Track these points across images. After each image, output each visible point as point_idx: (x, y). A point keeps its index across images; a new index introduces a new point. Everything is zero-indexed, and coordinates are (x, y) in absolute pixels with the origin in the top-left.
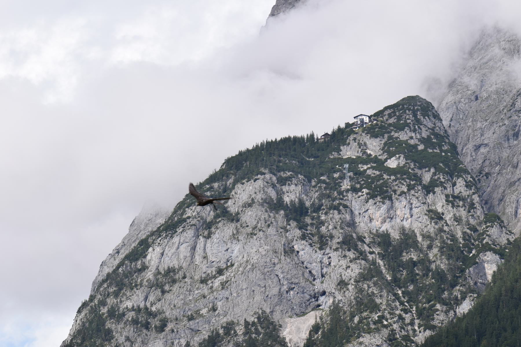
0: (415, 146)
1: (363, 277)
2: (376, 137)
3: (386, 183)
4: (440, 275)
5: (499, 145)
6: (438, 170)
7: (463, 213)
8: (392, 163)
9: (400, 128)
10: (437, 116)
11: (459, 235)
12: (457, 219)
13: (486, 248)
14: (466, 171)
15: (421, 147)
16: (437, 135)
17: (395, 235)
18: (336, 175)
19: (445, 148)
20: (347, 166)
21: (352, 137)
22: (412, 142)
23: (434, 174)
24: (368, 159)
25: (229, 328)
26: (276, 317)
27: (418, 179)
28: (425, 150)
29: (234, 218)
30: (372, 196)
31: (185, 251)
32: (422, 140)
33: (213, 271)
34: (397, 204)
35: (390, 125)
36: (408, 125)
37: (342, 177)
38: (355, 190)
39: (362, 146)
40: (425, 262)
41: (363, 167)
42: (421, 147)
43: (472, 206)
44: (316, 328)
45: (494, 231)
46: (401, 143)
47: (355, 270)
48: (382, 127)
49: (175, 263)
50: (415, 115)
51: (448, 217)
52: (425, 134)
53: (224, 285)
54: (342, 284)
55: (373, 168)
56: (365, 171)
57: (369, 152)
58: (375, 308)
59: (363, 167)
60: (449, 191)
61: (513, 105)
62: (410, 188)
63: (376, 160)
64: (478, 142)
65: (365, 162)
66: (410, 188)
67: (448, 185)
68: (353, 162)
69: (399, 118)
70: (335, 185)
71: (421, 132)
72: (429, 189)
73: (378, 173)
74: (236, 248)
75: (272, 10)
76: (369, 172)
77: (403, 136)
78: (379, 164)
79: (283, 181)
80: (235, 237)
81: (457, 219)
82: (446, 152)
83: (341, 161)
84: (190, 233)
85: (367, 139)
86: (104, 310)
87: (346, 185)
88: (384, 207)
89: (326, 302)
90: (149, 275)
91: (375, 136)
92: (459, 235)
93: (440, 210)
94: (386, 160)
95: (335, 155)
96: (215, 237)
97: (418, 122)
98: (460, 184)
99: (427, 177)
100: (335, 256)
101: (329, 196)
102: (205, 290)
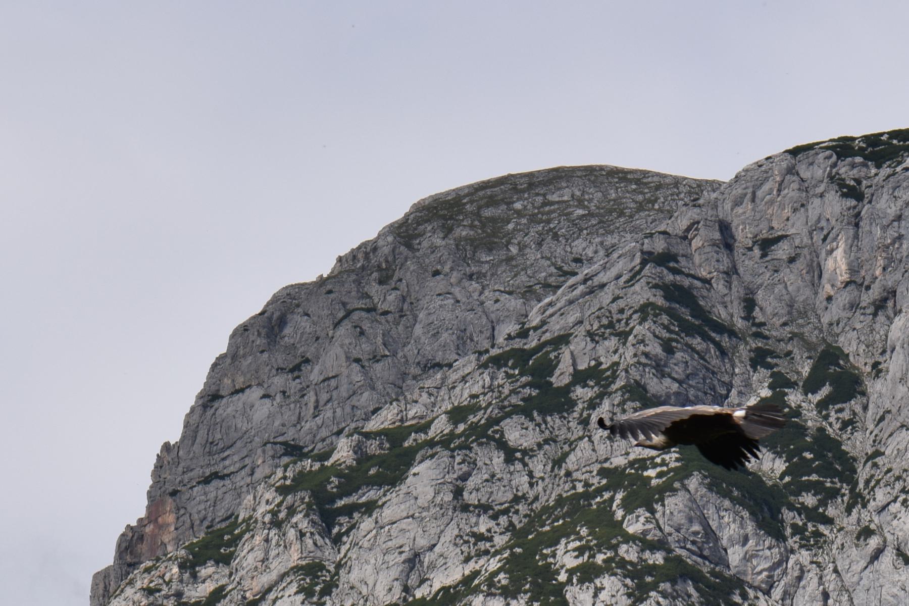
75: (210, 377)
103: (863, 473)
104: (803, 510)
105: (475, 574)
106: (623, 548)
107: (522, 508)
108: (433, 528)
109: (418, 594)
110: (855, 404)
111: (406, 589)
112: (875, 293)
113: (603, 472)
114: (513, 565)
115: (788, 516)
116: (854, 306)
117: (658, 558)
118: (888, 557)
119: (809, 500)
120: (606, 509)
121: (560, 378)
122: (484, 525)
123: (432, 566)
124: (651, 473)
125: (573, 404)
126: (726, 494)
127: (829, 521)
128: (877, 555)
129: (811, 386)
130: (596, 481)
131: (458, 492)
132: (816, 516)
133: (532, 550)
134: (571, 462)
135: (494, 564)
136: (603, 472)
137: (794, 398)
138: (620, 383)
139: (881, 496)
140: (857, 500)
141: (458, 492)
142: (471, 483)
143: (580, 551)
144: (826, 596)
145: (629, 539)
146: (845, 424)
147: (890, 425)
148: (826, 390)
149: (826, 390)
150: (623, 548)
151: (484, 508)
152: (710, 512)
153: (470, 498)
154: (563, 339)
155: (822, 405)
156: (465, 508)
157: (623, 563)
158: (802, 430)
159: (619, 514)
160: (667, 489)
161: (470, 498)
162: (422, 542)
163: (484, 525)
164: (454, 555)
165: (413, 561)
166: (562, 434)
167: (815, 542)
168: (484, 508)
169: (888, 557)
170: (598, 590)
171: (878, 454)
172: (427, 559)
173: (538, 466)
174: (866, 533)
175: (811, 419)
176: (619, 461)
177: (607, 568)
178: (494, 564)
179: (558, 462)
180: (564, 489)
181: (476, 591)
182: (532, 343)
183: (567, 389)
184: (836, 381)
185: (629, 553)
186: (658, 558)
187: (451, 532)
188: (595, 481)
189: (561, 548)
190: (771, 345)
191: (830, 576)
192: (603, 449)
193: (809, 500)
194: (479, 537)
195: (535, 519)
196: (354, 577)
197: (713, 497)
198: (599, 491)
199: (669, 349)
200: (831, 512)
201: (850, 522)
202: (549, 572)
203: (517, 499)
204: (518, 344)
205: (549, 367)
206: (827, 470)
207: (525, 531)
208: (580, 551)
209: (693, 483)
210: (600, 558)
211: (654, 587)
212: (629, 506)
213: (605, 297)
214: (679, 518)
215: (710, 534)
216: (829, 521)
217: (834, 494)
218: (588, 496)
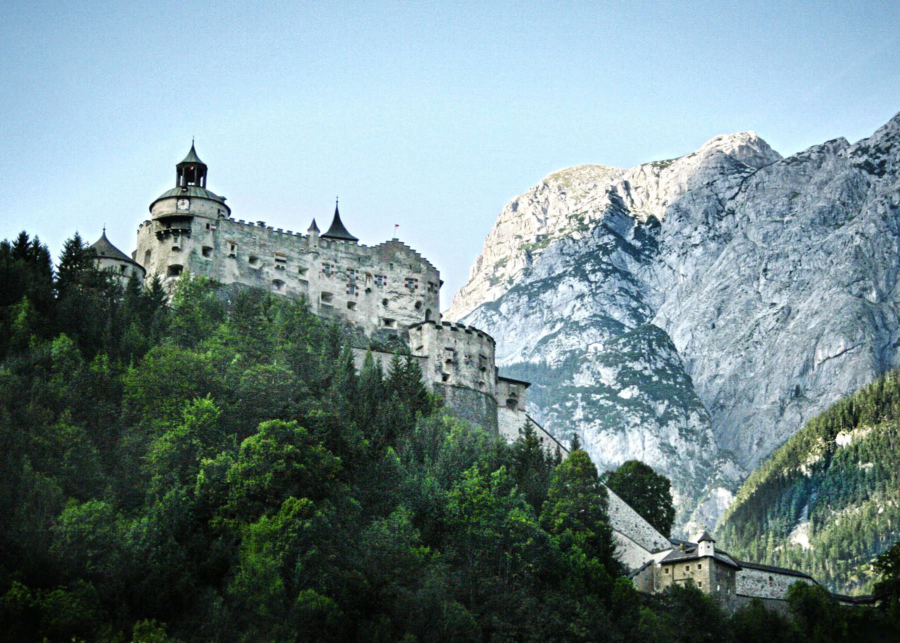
0: (650, 377)
2: (611, 366)
3: (619, 415)
5: (735, 377)
6: (672, 403)
8: (626, 394)
9: (636, 359)
10: (672, 347)
11: (692, 469)
12: (691, 454)
14: (700, 405)
15: (655, 378)
16: (671, 366)
18: (569, 404)
19: (680, 380)
20: (580, 395)
21: (585, 366)
22: (646, 373)
23: (668, 407)
24: (601, 389)
27: (652, 411)
28: (660, 381)
30: (605, 427)
32: (657, 371)
34: (629, 435)
35: (625, 354)
36: (643, 355)
37: (575, 407)
38: (587, 420)
39: (596, 375)
41: (595, 397)
42: (655, 378)
43: (705, 441)
46: (635, 373)
48: (616, 356)
50: (650, 346)
51: (681, 451)
52: (660, 365)
55: (607, 398)
56: (598, 401)
57: (602, 381)
59: (595, 397)
60: (683, 424)
61: (751, 335)
62: (644, 420)
63: (609, 390)
64: (714, 372)
65: (597, 391)
66: (644, 420)
67: (682, 419)
68: (587, 392)
69: (634, 347)
72: (662, 422)
73: (611, 403)
76: (602, 402)
77: (637, 366)
78: (613, 394)
81: (691, 454)
82: (681, 384)
83: (573, 390)
85: (600, 368)
87: (579, 414)
88: (617, 438)
91: (610, 365)
92: (692, 469)
93: (673, 444)
94: (620, 390)
95: (567, 383)
97: (653, 352)
98: (694, 417)
99: (661, 409)
101: (560, 425)
103: (660, 246)
104: (645, 255)
105: (566, 271)
106: (602, 266)
107: (577, 254)
108: (555, 259)
109: (552, 275)
110: (658, 228)
111: (549, 274)
112: (662, 201)
113: (597, 246)
114: (575, 269)
115: (643, 257)
116: (657, 204)
117: (611, 268)
118: (666, 267)
119: (647, 253)
120: (598, 255)
121: (586, 222)
122: (568, 258)
123: (556, 269)
124: (608, 246)
125: (589, 228)
126: (627, 252)
127: (652, 258)
128: (664, 266)
129: (647, 224)
130: (595, 248)
131: (562, 250)
132: (649, 257)
133: (580, 265)
134: (589, 243)
135: (571, 269)
136: (597, 246)
137: (643, 227)
138: (601, 224)
139: (664, 252)
140: (659, 253)
141: (562, 250)
142: (564, 248)
143: (592, 266)
144: (651, 276)
145: (604, 263)
146: (656, 234)
147: (666, 234)
148: (651, 225)
149: (651, 225)
150: (602, 266)
151: (568, 254)
152: (623, 256)
153: (564, 252)
154: (586, 212)
155: (650, 229)
156: (563, 254)
157: (602, 269)
158: (645, 235)
159: (601, 257)
160: (612, 251)
161: (564, 252)
162: (553, 263)
163: (568, 258)
164: (560, 265)
165: (551, 268)
166: (587, 236)
167: (649, 263)
168: (568, 254)
169: (666, 267)
170: (596, 276)
171: (663, 241)
172: (554, 267)
173: (581, 244)
174: (661, 261)
175: (647, 233)
176: (600, 243)
177: (599, 270)
178: (571, 269)
179: (586, 243)
180: (587, 250)
181: (567, 275)
182: (579, 213)
183: (587, 225)
184: (653, 222)
185: (603, 266)
186: (611, 268)
187: (560, 260)
188: (595, 248)
189: (587, 265)
190: (637, 213)
191: (652, 271)
192: (597, 240)
193: (647, 253)
194: (567, 262)
195: (581, 257)
196: (536, 271)
197: (623, 252)
198: (596, 251)
199: (612, 215)
200: (652, 255)
201: (657, 258)
202: (584, 271)
203: (576, 252)
204: (576, 213)
205: (582, 219)
206: (651, 245)
207: (578, 260)
208: (592, 266)
209: (619, 249)
210: (597, 268)
211: (610, 275)
212: (603, 255)
213: (596, 202)
214: (616, 258)
215: (623, 261)
216: (652, 258)
217: (653, 251)
218: (593, 252)
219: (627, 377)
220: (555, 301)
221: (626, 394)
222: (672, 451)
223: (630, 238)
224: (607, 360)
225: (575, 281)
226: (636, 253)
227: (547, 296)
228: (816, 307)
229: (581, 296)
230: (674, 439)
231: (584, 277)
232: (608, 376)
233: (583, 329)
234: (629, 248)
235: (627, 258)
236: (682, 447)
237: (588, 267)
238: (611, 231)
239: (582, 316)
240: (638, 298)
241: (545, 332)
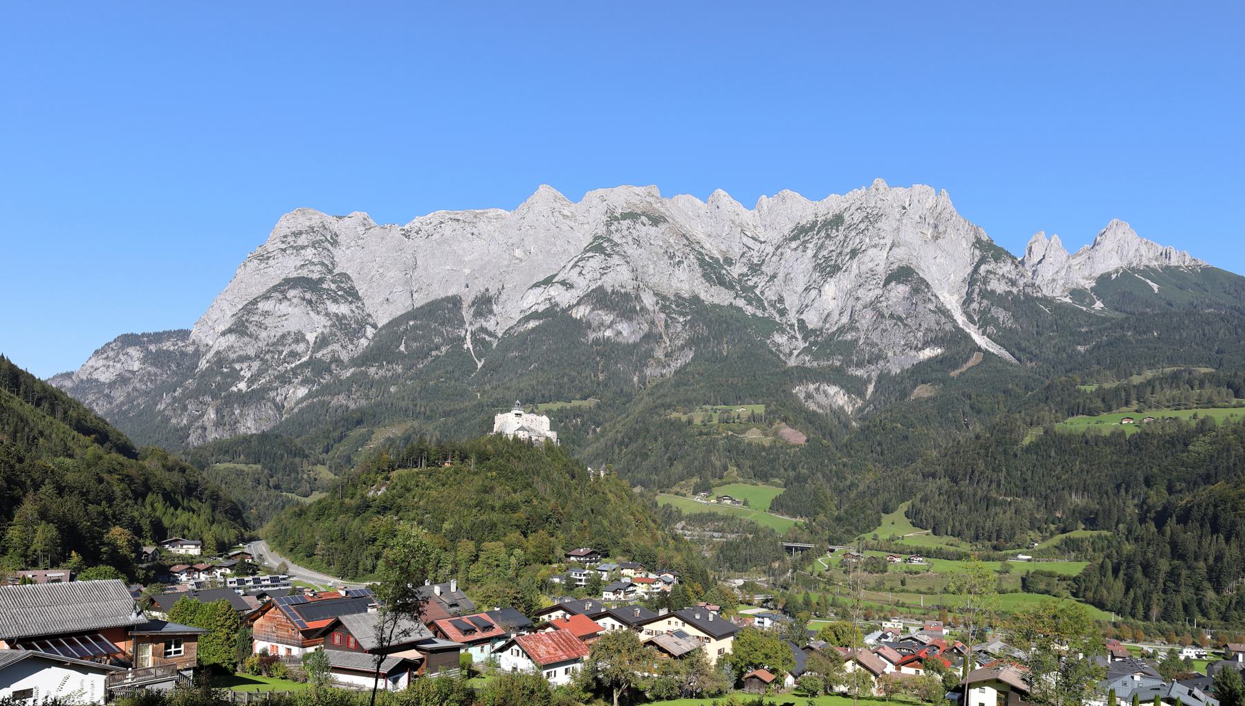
1: (332, 326)
4: (354, 329)
7: (360, 312)
8: (339, 293)
9: (342, 283)
13: (368, 324)
17: (340, 314)
25: (289, 333)
26: (303, 332)
29: (289, 300)
31: (272, 306)
33: (282, 314)
40: (350, 325)
44: (317, 338)
45: (370, 319)
47: (329, 323)
49: (268, 309)
53: (286, 320)
54: (324, 326)
58: (336, 336)
70: (321, 296)
71: (352, 288)
72: (351, 303)
74: (290, 309)
78: (335, 293)
79: (305, 292)
80: (290, 306)
84: (274, 301)
86: (244, 319)
87: (325, 297)
89: (319, 331)
90: (260, 311)
96: (283, 304)
99: (350, 299)
100: (322, 318)
102: (279, 319)
219: (340, 289)
220: (306, 254)
221: (339, 293)
222: (353, 312)
223: (329, 238)
224: (333, 282)
225: (313, 249)
226: (332, 245)
227: (303, 252)
228: (393, 275)
229: (315, 254)
230: (354, 308)
231: (316, 249)
232: (333, 286)
233: (316, 265)
234: (329, 242)
235: (329, 245)
236: (356, 311)
237: (317, 246)
238: (323, 236)
239: (315, 260)
240: (333, 258)
241: (303, 263)
